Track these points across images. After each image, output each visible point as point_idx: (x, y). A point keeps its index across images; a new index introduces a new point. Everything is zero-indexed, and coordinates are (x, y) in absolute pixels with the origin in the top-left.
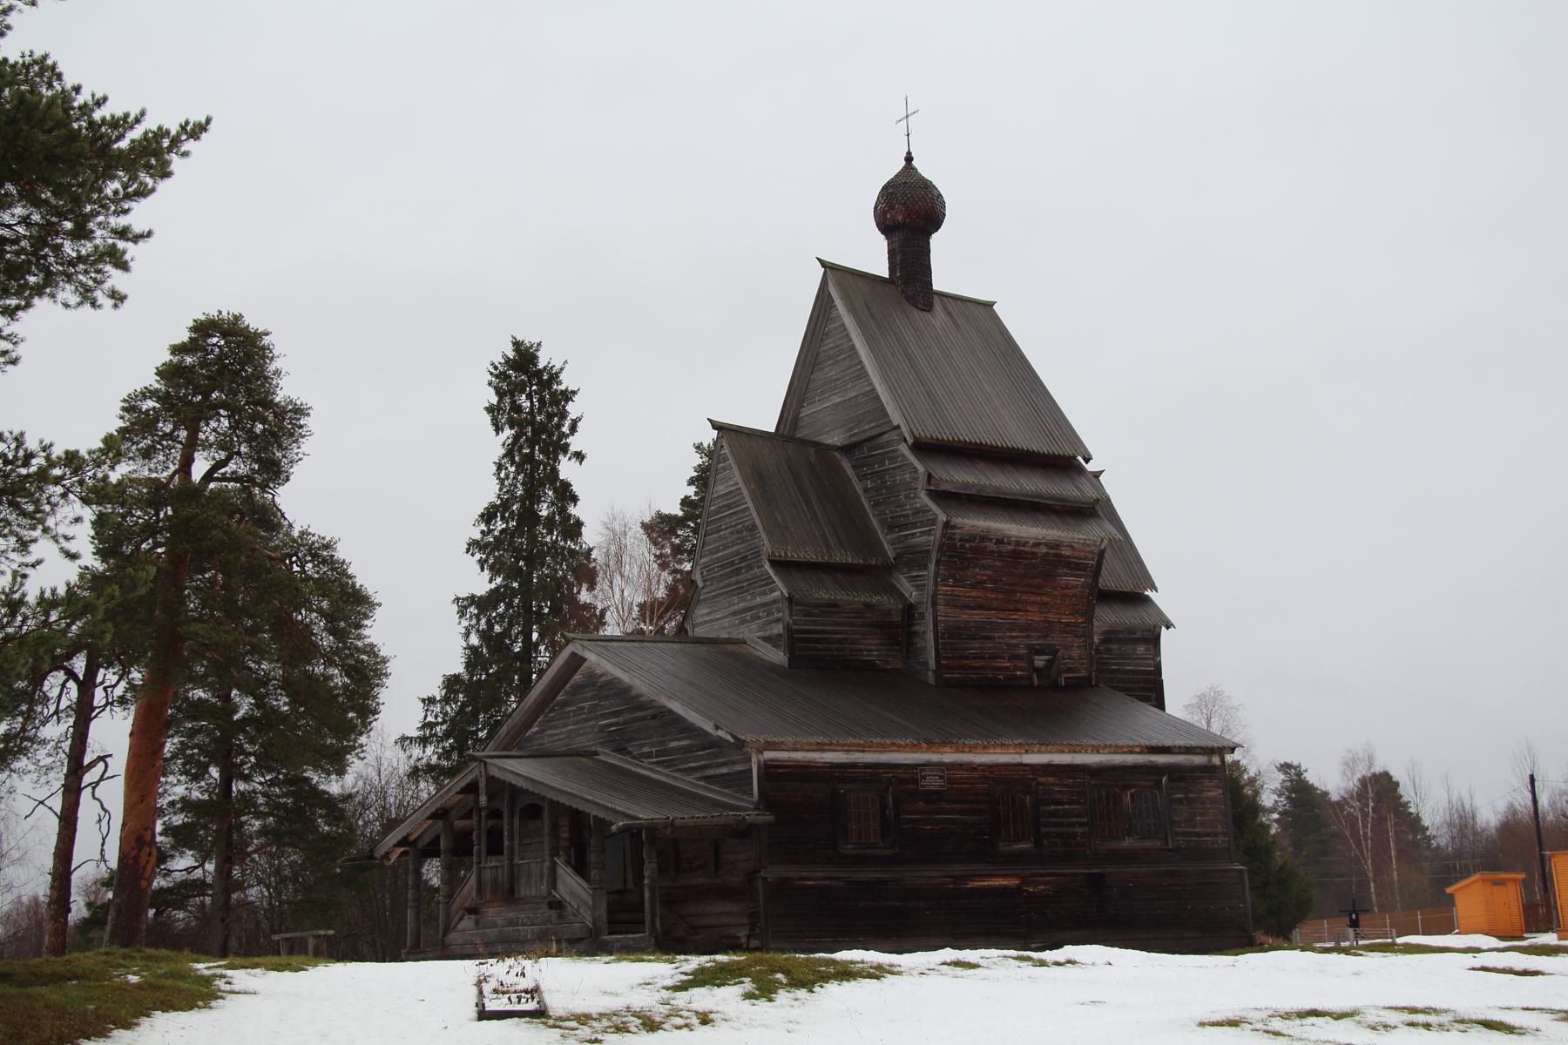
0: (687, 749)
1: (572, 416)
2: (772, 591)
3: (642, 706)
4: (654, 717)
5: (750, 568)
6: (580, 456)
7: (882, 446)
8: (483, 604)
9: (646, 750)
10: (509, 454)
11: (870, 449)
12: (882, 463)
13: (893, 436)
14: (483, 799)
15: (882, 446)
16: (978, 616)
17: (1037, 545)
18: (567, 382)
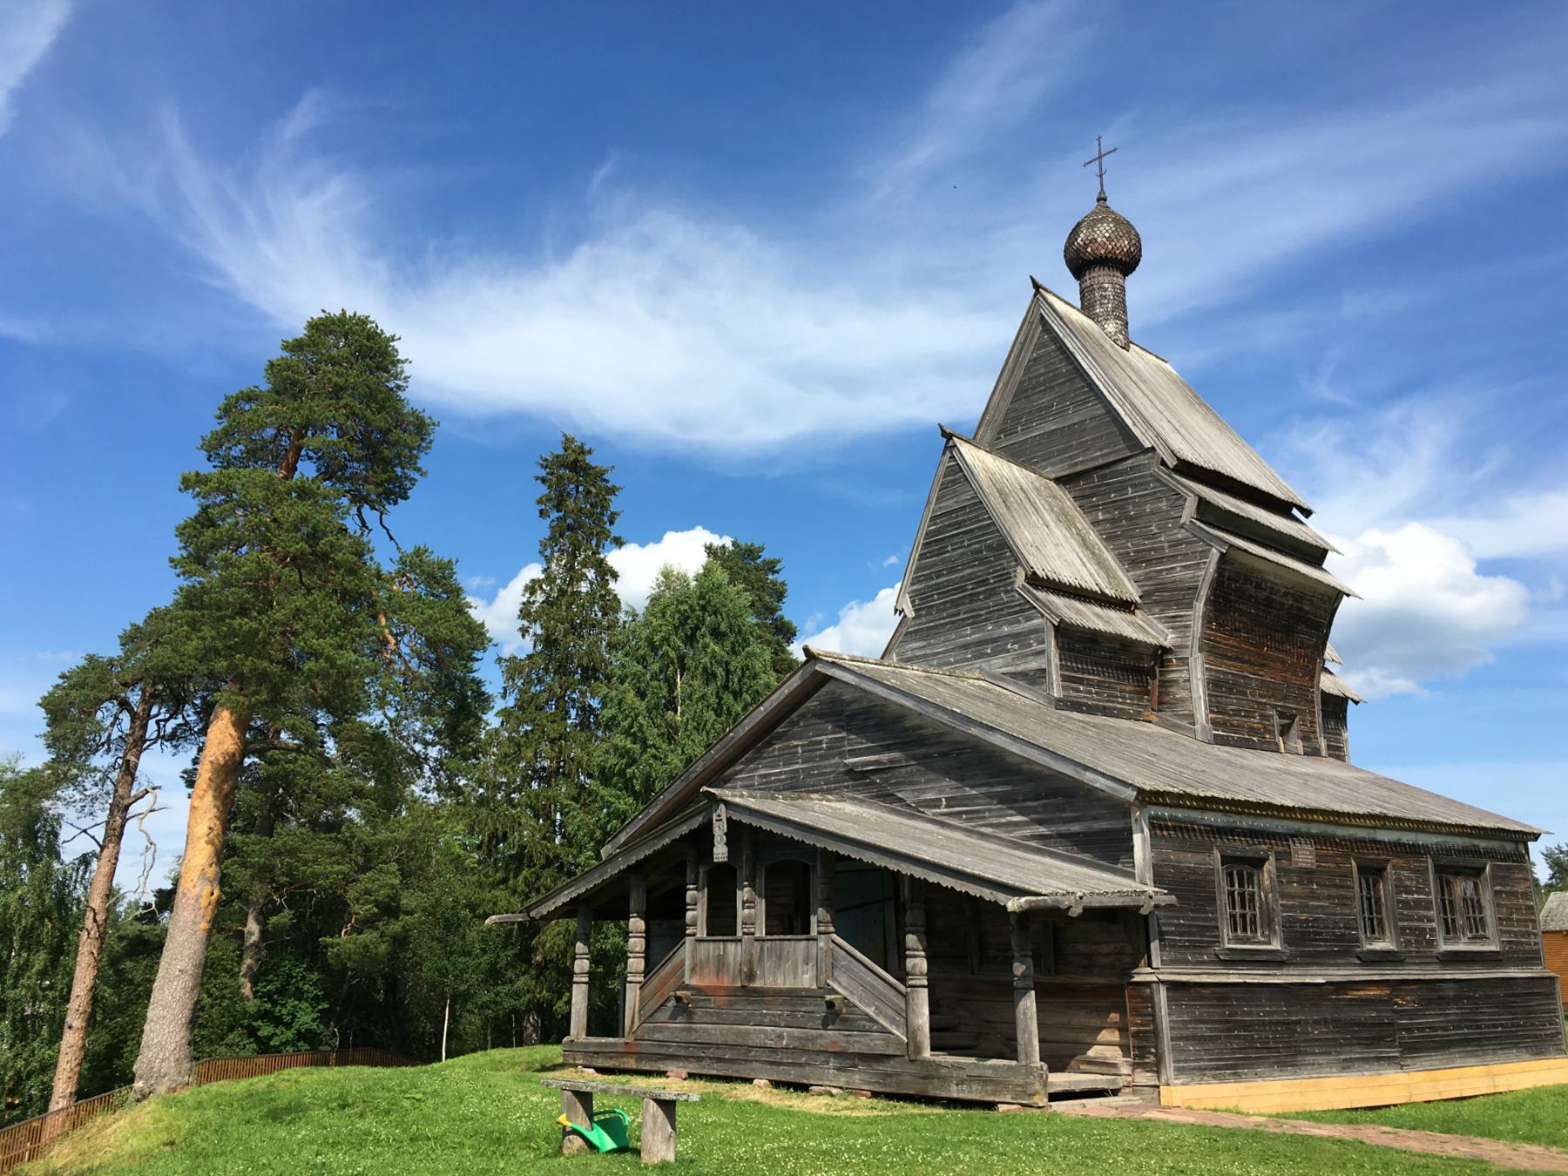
1: (613, 508)
2: (1029, 619)
4: (943, 755)
5: (992, 593)
7: (1122, 473)
9: (929, 796)
11: (1105, 477)
12: (1122, 489)
13: (1143, 459)
15: (1122, 473)
17: (1286, 595)
18: (613, 479)
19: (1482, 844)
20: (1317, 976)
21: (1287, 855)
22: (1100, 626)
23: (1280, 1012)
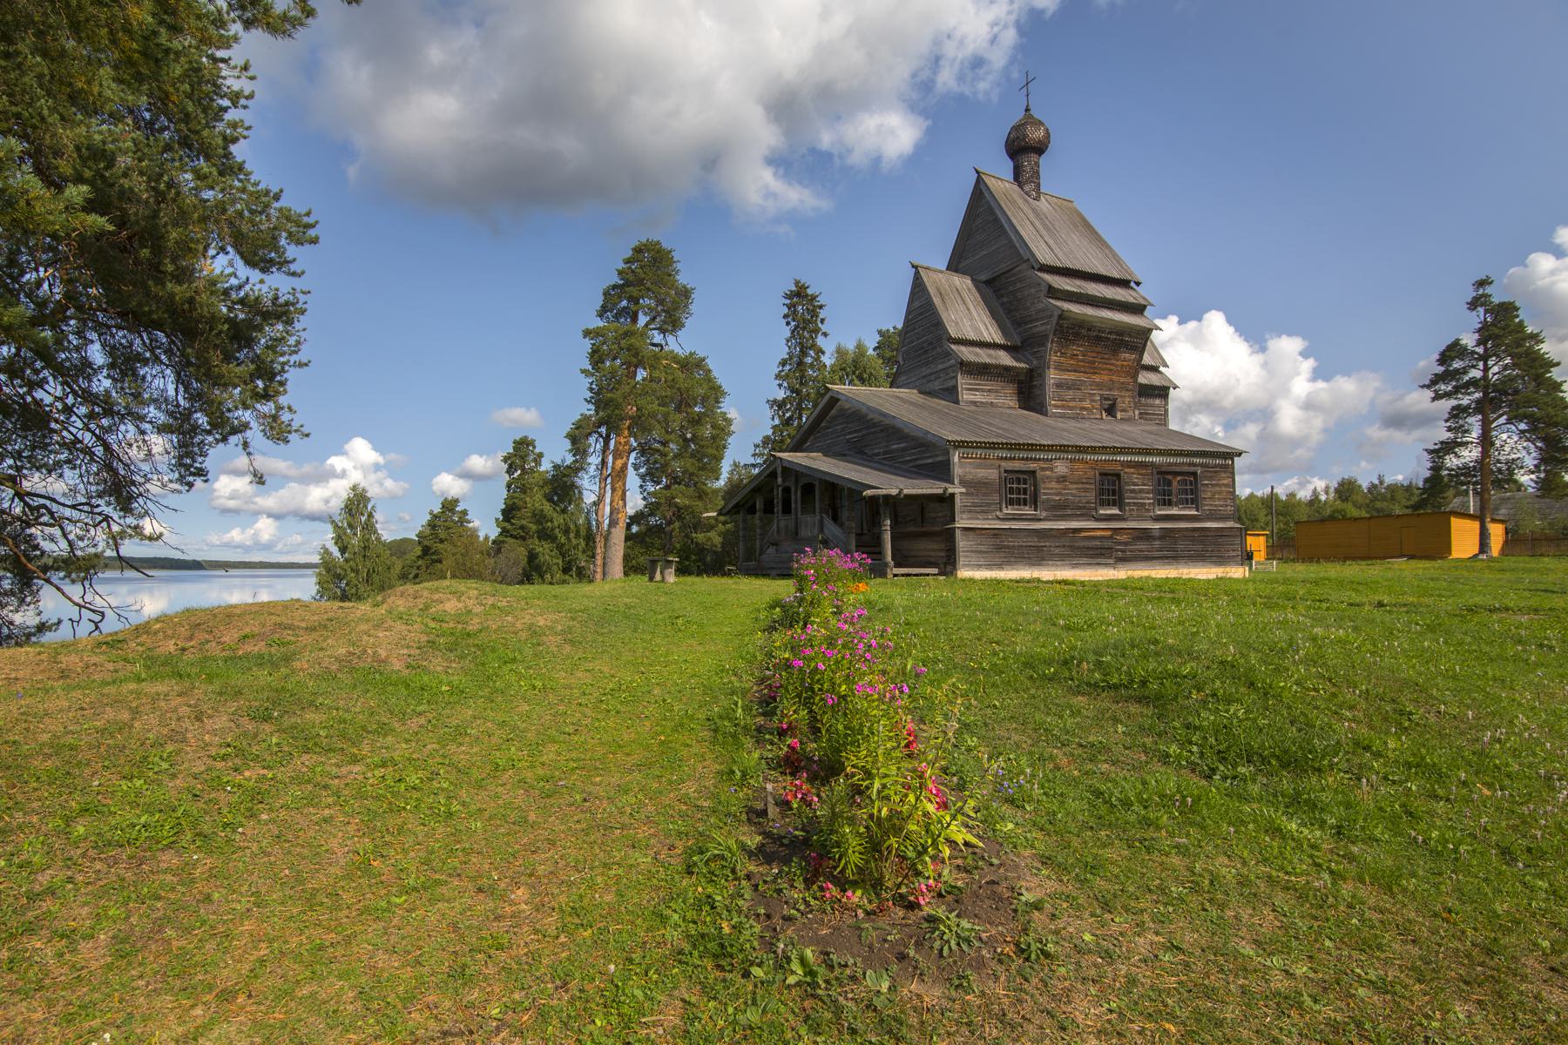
0: (904, 449)
3: (874, 425)
6: (825, 335)
8: (780, 405)
10: (793, 336)
13: (1024, 266)
14: (780, 480)
16: (1072, 376)
18: (821, 300)
19: (1197, 460)
20: (1062, 525)
21: (1051, 469)
22: (988, 361)
23: (1034, 541)
